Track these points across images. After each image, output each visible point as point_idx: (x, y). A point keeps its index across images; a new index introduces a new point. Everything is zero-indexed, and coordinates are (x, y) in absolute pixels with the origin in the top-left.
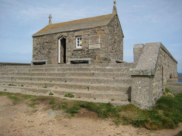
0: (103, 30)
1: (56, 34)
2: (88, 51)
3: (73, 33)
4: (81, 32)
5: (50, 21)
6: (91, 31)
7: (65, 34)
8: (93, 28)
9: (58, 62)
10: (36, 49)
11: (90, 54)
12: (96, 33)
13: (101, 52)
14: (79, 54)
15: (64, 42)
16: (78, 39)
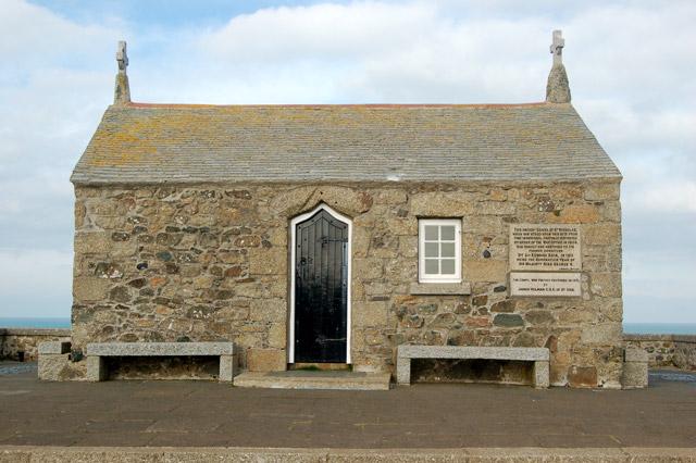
2: (506, 306)
4: (461, 196)
5: (123, 85)
6: (523, 200)
9: (288, 358)
10: (106, 268)
11: (522, 324)
12: (557, 213)
13: (588, 315)
14: (443, 316)
16: (431, 233)
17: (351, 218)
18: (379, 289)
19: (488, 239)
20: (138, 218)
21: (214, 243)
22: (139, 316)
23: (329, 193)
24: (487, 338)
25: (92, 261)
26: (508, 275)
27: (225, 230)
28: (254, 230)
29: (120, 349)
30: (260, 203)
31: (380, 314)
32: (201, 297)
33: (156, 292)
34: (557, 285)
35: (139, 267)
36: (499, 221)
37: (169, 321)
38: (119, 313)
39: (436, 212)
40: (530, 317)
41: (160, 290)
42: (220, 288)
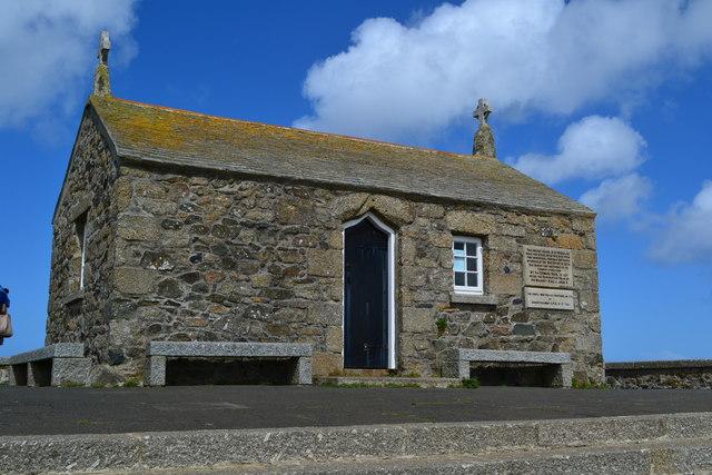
0: (582, 235)
1: (334, 188)
2: (521, 317)
3: (438, 210)
6: (530, 226)
7: (397, 208)
8: (542, 214)
10: (154, 257)
14: (474, 324)
15: (366, 245)
17: (396, 228)
18: (425, 296)
19: (508, 257)
20: (193, 206)
21: (272, 240)
22: (192, 314)
23: (382, 202)
24: (506, 344)
25: (139, 248)
26: (523, 289)
27: (284, 228)
28: (311, 230)
29: (193, 348)
30: (318, 204)
31: (422, 321)
32: (259, 296)
33: (211, 289)
34: (558, 300)
35: (193, 260)
36: (514, 241)
37: (225, 321)
38: (168, 310)
39: (468, 229)
40: (541, 327)
41: (215, 286)
42: (278, 288)
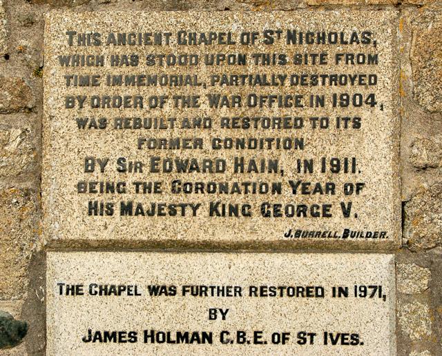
26: (37, 263)
